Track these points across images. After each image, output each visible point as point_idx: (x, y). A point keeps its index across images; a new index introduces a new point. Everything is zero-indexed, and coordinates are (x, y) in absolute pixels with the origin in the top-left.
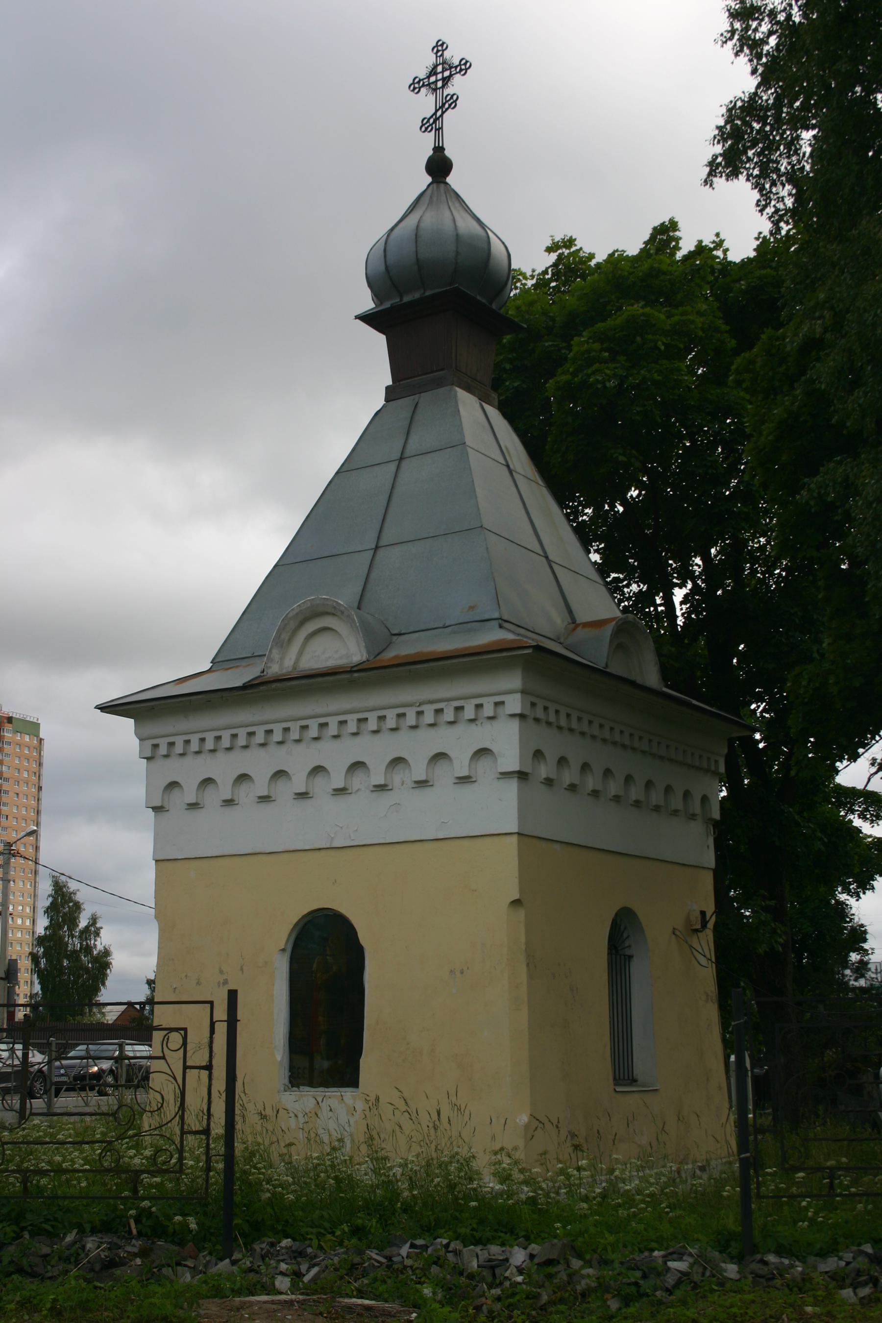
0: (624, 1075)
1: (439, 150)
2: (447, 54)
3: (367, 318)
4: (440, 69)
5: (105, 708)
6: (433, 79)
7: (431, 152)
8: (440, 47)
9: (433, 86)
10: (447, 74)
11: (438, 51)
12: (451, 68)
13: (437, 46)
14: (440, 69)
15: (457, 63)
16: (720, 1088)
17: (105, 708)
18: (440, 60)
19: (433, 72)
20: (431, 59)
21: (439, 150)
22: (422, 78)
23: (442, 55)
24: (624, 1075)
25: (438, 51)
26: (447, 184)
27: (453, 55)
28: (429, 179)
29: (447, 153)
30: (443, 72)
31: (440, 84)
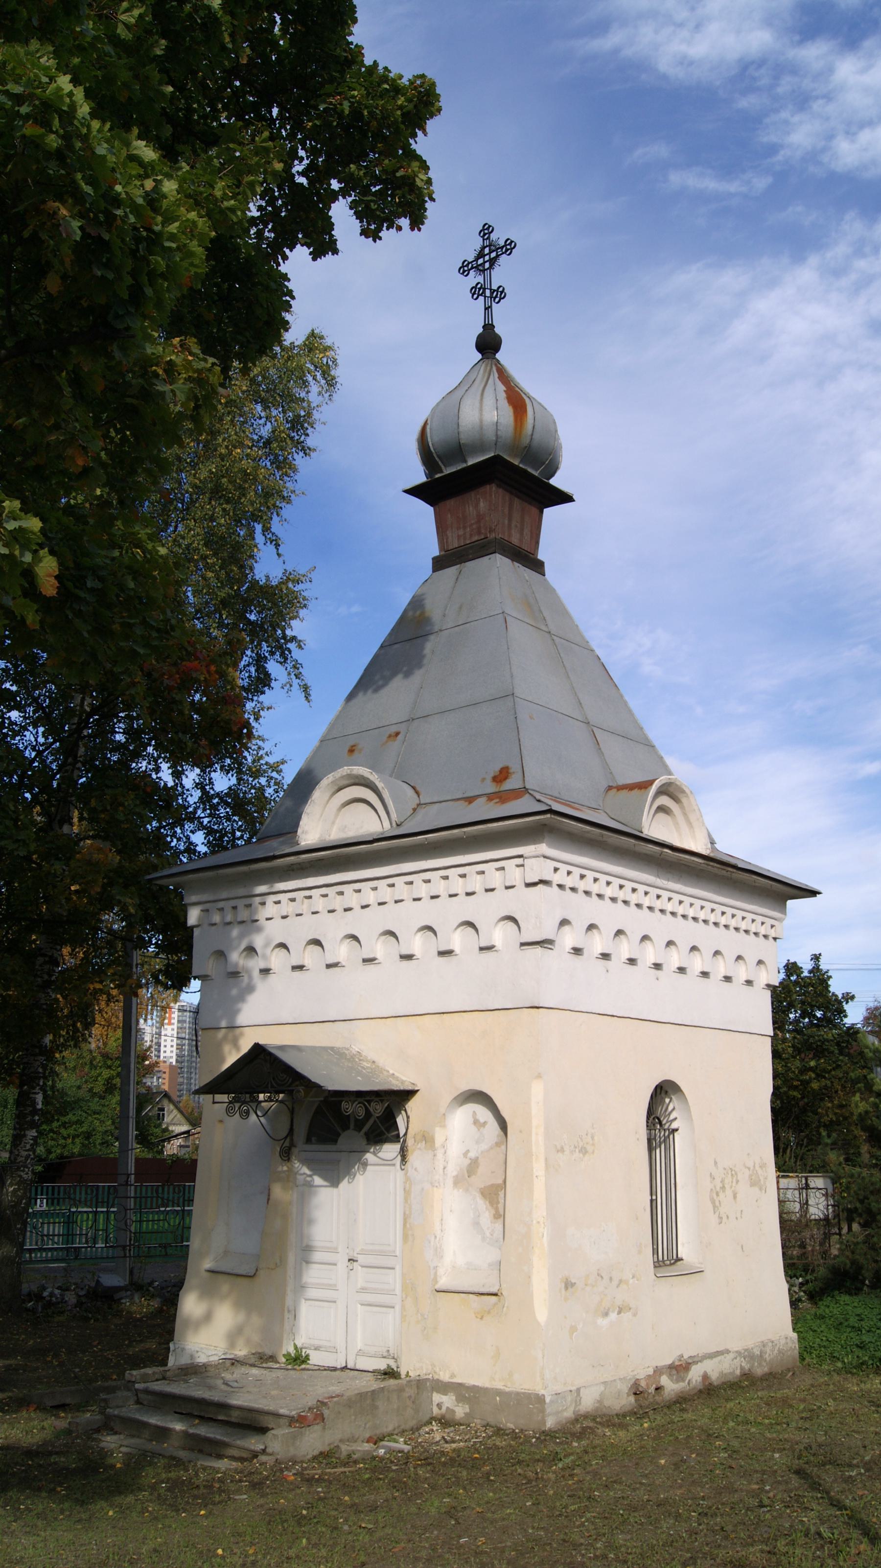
0: (666, 1260)
1: (488, 327)
2: (493, 236)
3: (415, 491)
4: (487, 251)
5: (813, 893)
6: (493, 255)
7: (481, 330)
8: (486, 231)
9: (481, 268)
10: (493, 255)
11: (485, 234)
12: (477, 268)
13: (483, 230)
14: (487, 251)
15: (471, 272)
16: (683, 1244)
17: (813, 893)
18: (487, 243)
19: (481, 255)
20: (478, 243)
21: (488, 327)
22: (470, 260)
23: (489, 238)
24: (666, 1260)
25: (485, 234)
26: (498, 361)
27: (499, 237)
28: (479, 356)
29: (497, 330)
30: (485, 262)
31: (487, 265)
